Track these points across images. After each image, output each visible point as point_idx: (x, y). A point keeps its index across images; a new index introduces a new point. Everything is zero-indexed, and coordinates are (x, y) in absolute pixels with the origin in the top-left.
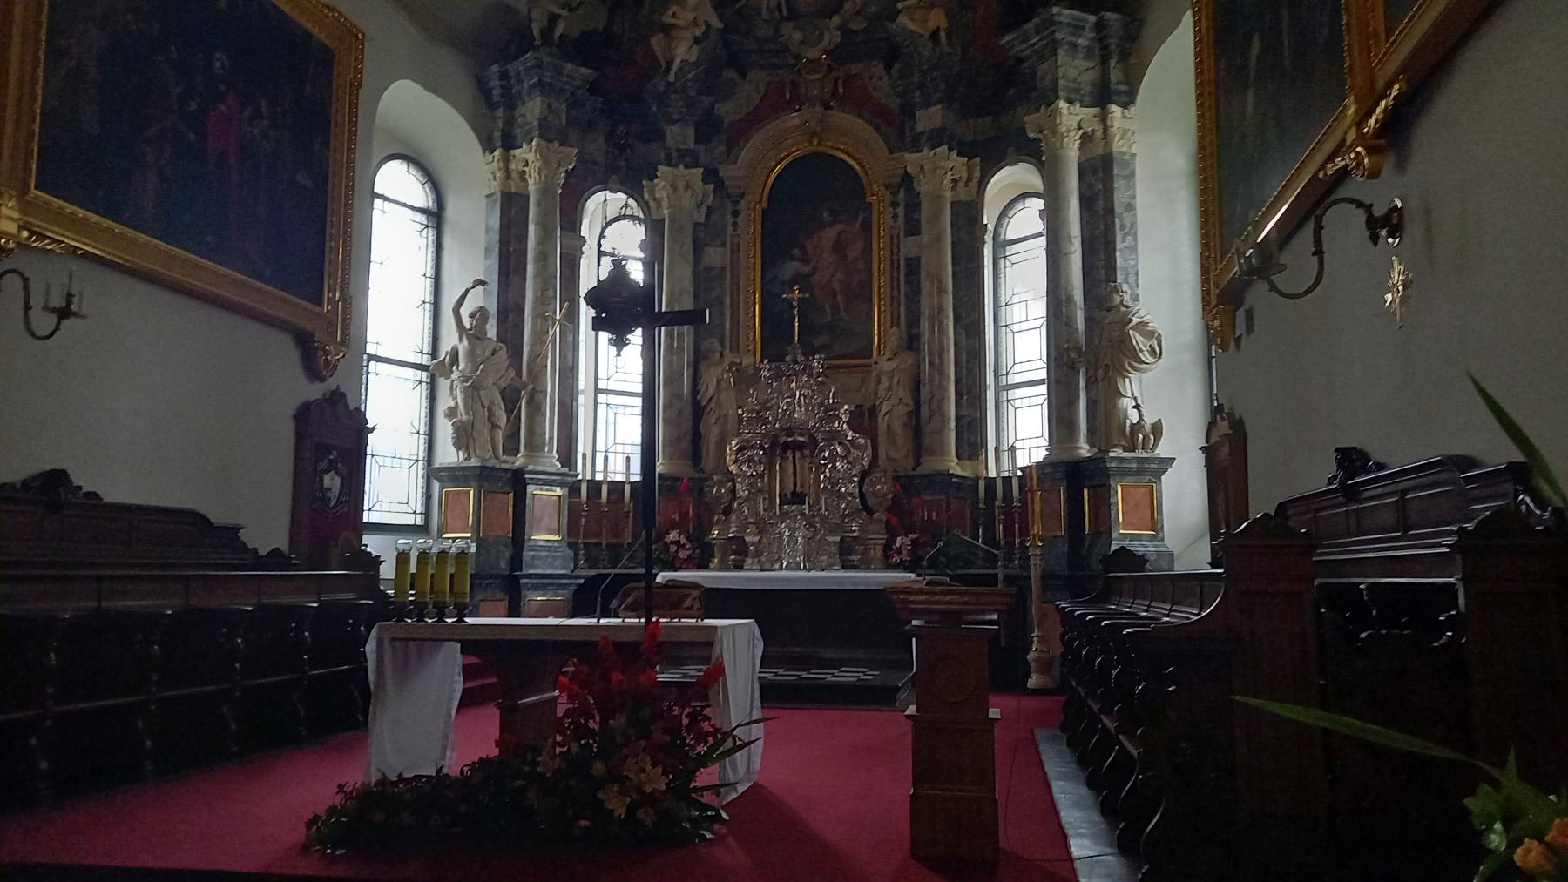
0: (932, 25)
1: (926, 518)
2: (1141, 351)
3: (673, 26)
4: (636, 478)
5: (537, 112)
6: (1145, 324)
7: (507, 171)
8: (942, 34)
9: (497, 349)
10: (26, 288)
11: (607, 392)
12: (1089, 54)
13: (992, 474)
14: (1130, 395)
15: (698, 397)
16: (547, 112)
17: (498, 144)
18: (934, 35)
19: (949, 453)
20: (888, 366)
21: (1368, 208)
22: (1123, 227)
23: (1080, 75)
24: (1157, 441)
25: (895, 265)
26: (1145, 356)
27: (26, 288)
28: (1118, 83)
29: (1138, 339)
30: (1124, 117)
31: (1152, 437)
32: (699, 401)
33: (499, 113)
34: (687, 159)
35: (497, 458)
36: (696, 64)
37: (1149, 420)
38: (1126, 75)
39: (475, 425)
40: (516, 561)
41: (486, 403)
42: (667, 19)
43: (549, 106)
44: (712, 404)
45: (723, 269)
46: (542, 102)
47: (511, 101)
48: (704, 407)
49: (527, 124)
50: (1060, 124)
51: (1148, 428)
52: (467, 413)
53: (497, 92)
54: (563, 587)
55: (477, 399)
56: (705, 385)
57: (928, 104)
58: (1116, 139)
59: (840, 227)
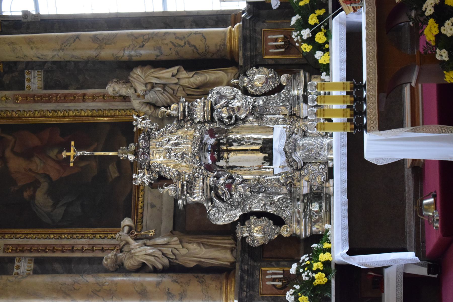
1: (283, 50)
15: (160, 267)
19: (224, 33)
20: (141, 88)
25: (49, 99)
32: (164, 266)
44: (168, 251)
48: (170, 262)
56: (148, 257)
59: (8, 153)
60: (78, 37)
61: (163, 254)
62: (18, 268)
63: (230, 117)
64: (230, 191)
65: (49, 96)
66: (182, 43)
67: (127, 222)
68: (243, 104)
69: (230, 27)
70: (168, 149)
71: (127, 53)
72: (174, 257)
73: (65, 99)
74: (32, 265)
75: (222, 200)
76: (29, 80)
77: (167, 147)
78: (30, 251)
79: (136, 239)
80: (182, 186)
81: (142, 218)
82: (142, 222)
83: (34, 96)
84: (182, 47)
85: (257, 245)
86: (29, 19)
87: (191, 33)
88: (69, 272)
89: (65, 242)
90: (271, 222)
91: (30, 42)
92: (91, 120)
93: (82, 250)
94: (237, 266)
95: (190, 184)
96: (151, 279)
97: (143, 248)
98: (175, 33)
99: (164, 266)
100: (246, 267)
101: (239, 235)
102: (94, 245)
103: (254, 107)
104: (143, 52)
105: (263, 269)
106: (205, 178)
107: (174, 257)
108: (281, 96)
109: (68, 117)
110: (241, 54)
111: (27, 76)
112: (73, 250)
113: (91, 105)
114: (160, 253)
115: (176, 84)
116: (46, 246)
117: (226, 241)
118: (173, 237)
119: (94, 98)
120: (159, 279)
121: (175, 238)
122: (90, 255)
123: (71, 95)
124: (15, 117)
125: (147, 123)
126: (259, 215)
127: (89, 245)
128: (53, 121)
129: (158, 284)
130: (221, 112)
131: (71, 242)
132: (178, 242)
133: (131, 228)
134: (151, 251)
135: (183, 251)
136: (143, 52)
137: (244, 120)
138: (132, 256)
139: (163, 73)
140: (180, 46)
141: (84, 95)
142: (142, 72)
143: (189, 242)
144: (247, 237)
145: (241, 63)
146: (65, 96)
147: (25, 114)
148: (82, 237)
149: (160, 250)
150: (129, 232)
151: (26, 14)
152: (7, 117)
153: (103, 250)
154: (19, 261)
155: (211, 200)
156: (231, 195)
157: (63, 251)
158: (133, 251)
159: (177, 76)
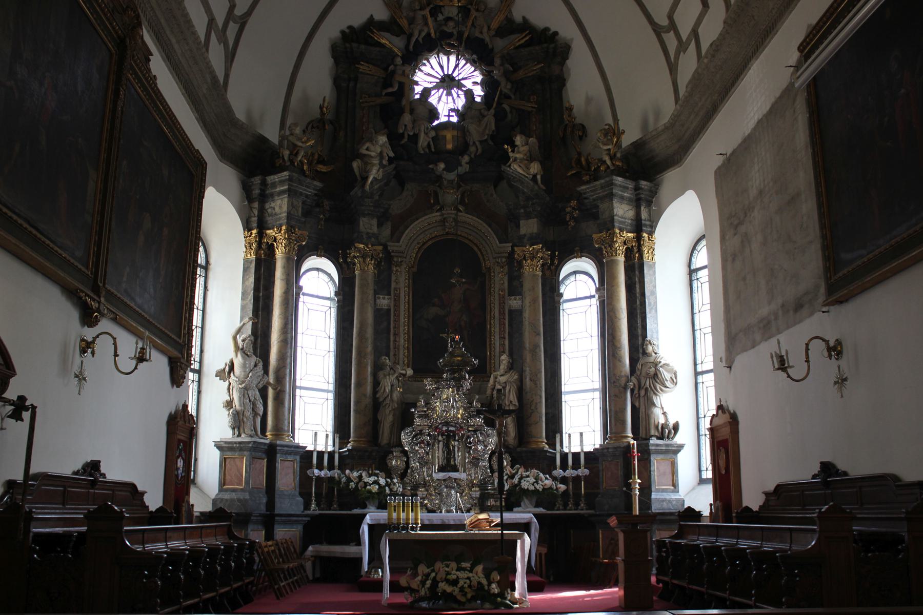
0: (532, 171)
2: (667, 380)
3: (365, 155)
4: (330, 449)
5: (285, 208)
6: (668, 365)
7: (260, 244)
8: (539, 177)
9: (257, 362)
10: (115, 344)
11: (301, 388)
12: (630, 201)
13: (566, 450)
14: (660, 406)
15: (377, 396)
16: (291, 208)
17: (255, 225)
18: (535, 176)
19: (541, 437)
20: (503, 379)
21: (827, 342)
22: (650, 304)
23: (625, 213)
24: (675, 433)
25: (502, 313)
26: (668, 384)
27: (115, 344)
28: (645, 220)
29: (667, 375)
30: (649, 239)
31: (673, 431)
32: (378, 398)
33: (256, 205)
34: (373, 239)
35: (257, 435)
36: (381, 180)
37: (671, 422)
38: (650, 215)
39: (245, 413)
40: (271, 504)
41: (252, 399)
42: (363, 151)
43: (292, 204)
44: (388, 401)
45: (389, 310)
46: (288, 201)
47: (264, 197)
48: (381, 402)
49: (276, 214)
50: (616, 241)
51: (671, 426)
52: (240, 405)
53: (256, 192)
54: (297, 522)
55: (247, 396)
56: (383, 388)
57: (528, 216)
58: (646, 252)
60: (539, 334)
61: (385, 398)
62: (384, 298)
63: (470, 443)
64: (420, 443)
65: (504, 313)
66: (533, 407)
67: (410, 372)
68: (479, 451)
69: (546, 441)
70: (450, 401)
71: (528, 369)
72: (384, 405)
73: (502, 324)
74: (386, 308)
75: (413, 438)
76: (515, 299)
77: (452, 400)
78: (395, 305)
79: (397, 378)
80: (425, 411)
81: (418, 381)
82: (415, 381)
83: (504, 303)
84: (530, 408)
85: (388, 461)
86: (556, 298)
87: (541, 413)
88: (376, 332)
89: (401, 329)
90: (402, 471)
91: (534, 301)
92: (488, 343)
93: (395, 341)
94: (376, 448)
95: (426, 416)
96: (369, 389)
97: (390, 384)
98: (541, 402)
99: (378, 398)
100: (374, 454)
101: (394, 449)
102: (399, 349)
103: (478, 459)
104: (528, 379)
105: (374, 465)
106: (430, 427)
107: (384, 405)
108: (489, 478)
109: (490, 327)
110: (524, 449)
111: (518, 297)
112: (395, 334)
113: (497, 344)
114: (386, 396)
115: (506, 405)
116: (399, 316)
117: (395, 440)
118: (397, 404)
119: (502, 345)
120: (368, 395)
121: (396, 406)
122: (392, 347)
123: (504, 328)
124: (490, 290)
125: (467, 386)
126: (407, 463)
127: (399, 346)
128: (488, 317)
129: (365, 395)
130: (474, 437)
131: (402, 334)
132: (394, 408)
133: (404, 375)
134: (387, 391)
135: (387, 411)
136: (528, 379)
137: (469, 452)
138: (385, 376)
139: (513, 394)
140: (531, 406)
141: (504, 338)
142: (515, 380)
143: (394, 415)
144: (393, 455)
145: (519, 449)
146: (504, 324)
147: (492, 297)
148: (405, 341)
149: (388, 395)
150: (401, 374)
151: (561, 295)
152: (491, 285)
153: (395, 355)
154: (388, 299)
155: (414, 431)
156: (417, 445)
157: (395, 327)
158: (387, 377)
159: (511, 405)
